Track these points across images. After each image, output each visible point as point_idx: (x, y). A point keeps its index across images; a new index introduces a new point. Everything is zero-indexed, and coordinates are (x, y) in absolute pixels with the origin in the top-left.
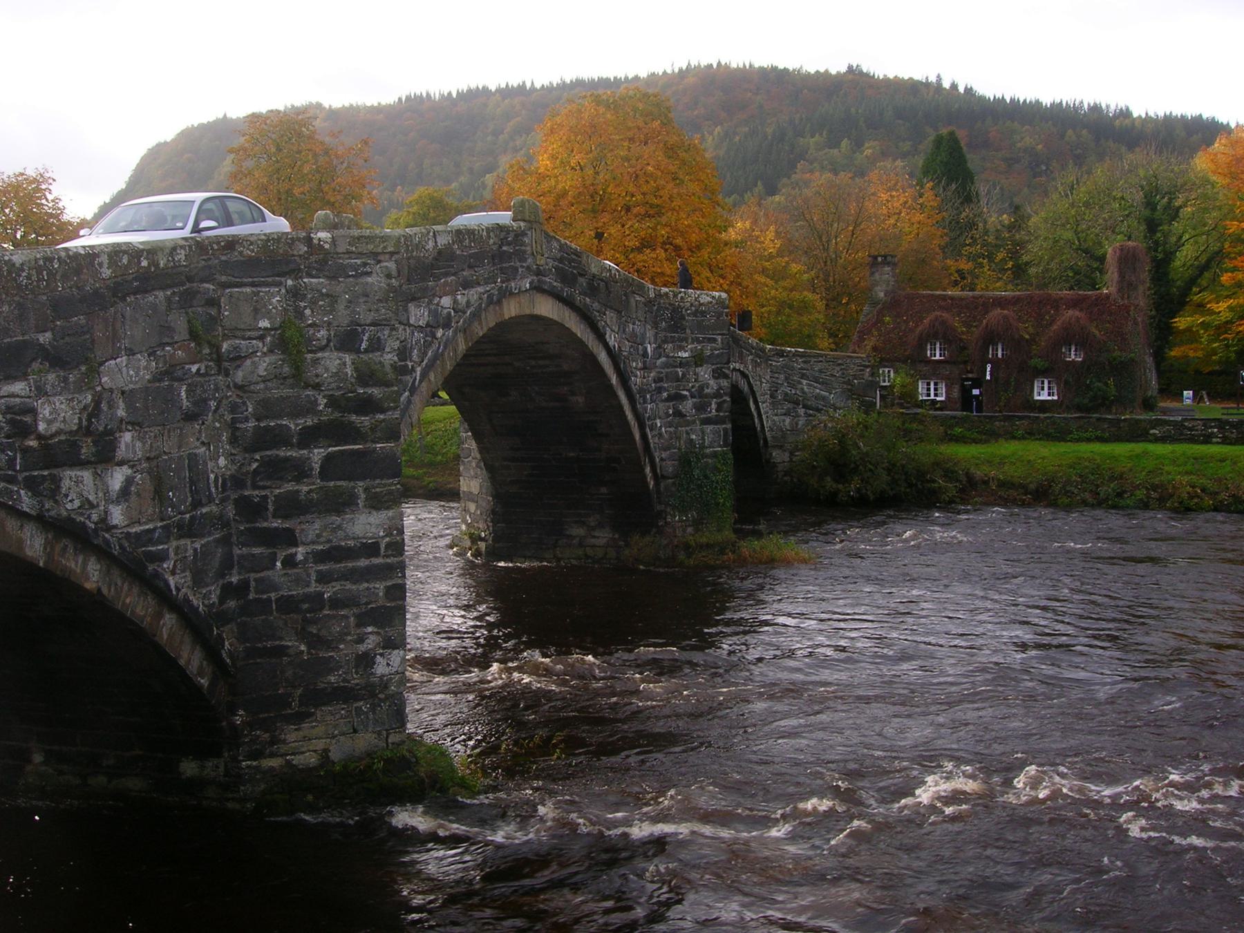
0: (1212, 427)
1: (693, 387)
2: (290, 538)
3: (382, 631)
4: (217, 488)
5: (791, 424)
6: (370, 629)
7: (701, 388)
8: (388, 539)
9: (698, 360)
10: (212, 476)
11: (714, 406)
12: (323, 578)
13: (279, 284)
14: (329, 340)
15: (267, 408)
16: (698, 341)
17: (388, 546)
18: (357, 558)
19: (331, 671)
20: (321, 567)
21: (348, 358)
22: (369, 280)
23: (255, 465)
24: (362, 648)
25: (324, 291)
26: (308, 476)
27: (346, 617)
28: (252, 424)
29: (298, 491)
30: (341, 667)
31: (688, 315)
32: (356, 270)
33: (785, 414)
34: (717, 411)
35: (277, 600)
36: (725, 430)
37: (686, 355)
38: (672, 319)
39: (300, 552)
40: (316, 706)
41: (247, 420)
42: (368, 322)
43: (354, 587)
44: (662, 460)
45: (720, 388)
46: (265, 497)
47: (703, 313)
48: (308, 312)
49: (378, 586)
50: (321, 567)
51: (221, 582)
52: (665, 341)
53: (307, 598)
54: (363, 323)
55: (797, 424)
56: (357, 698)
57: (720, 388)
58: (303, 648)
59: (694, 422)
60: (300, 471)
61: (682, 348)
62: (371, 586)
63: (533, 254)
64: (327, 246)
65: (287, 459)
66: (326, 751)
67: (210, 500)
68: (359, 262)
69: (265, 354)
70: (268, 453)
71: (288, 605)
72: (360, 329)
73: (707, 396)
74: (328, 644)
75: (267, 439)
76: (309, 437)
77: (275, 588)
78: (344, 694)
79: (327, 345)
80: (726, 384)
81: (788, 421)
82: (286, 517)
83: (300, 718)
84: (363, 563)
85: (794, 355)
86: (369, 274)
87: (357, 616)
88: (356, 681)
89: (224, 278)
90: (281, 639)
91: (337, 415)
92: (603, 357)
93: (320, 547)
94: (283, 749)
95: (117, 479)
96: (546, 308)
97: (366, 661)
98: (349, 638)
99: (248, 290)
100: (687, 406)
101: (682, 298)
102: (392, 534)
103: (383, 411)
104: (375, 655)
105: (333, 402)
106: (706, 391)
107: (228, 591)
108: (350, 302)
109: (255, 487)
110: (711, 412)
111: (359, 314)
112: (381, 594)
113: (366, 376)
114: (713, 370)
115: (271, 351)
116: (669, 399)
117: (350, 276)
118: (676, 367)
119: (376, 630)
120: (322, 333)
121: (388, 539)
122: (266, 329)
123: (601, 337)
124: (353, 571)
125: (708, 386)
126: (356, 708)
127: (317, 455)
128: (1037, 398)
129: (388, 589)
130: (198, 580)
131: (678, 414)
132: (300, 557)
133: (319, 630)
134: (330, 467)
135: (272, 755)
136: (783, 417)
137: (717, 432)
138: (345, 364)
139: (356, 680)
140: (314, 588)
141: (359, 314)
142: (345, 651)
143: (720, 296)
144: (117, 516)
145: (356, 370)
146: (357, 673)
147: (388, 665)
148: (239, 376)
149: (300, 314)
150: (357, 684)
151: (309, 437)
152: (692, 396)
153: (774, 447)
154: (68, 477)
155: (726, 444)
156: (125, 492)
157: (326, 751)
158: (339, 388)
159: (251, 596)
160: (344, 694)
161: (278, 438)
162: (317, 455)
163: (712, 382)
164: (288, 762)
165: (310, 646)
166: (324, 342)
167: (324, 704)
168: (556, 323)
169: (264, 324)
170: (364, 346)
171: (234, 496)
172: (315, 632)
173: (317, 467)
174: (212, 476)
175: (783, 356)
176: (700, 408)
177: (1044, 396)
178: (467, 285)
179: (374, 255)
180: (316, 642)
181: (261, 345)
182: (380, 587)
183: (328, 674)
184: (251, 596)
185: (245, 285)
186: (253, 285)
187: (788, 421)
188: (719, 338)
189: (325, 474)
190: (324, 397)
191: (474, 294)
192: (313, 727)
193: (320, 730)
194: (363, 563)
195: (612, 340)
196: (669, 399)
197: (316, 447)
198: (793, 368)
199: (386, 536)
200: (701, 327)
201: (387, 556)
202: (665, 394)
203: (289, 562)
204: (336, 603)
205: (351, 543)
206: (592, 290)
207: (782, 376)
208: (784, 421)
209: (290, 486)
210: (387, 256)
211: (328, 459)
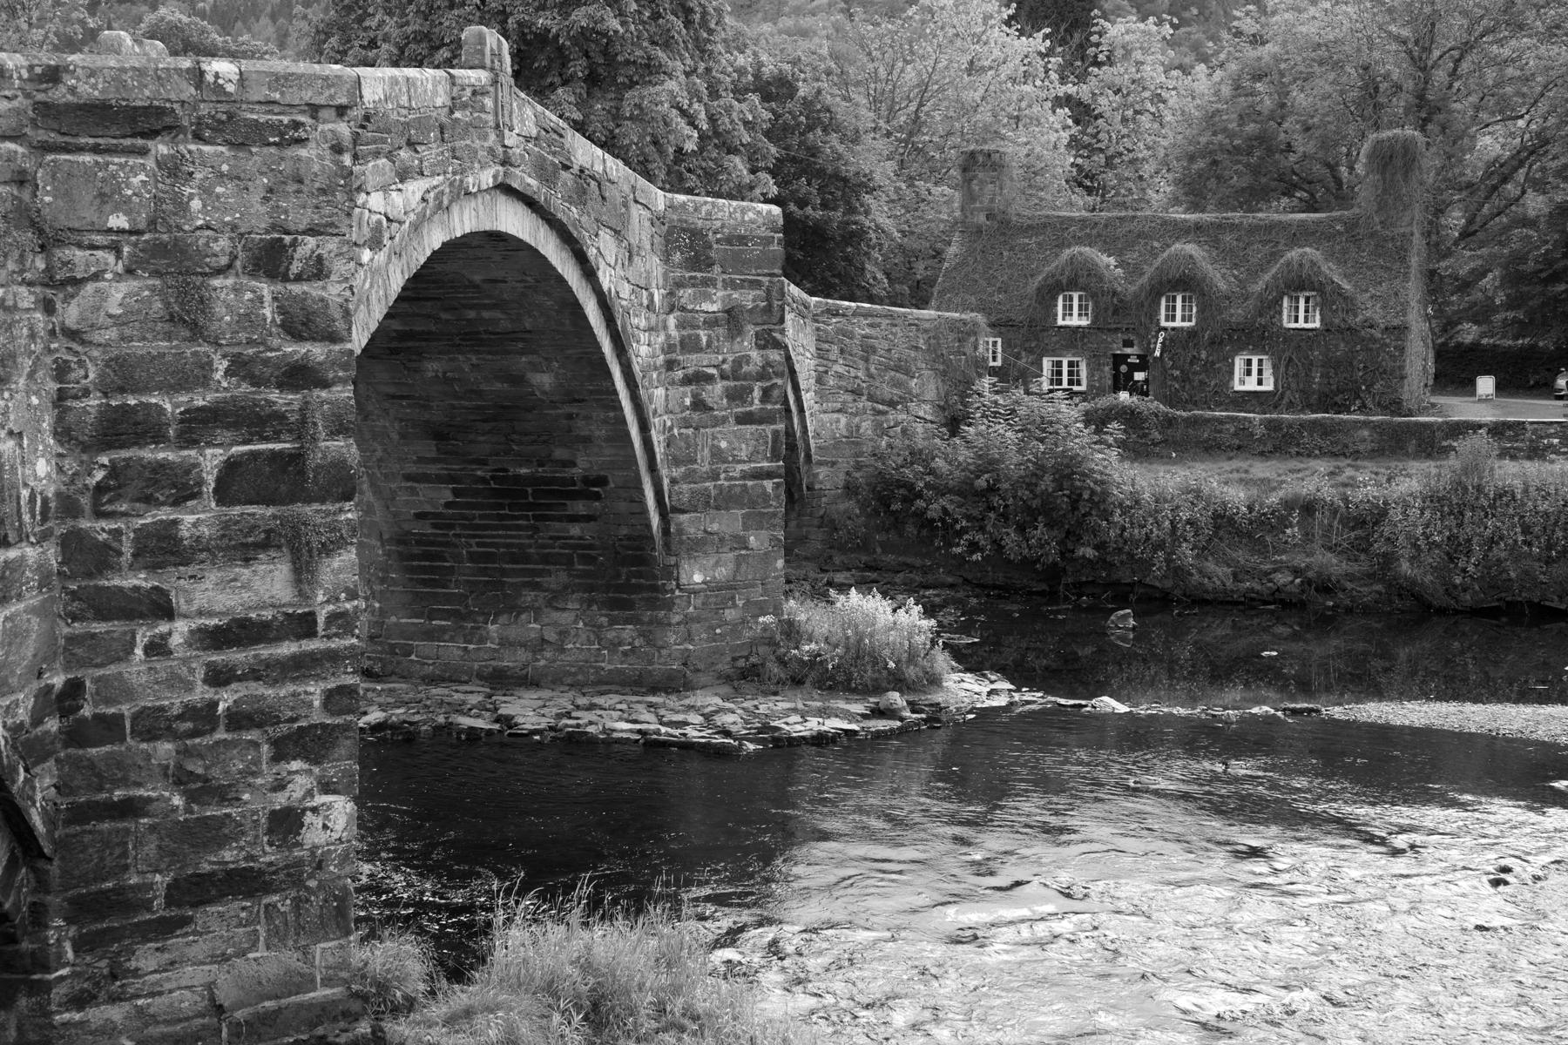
0: (1549, 436)
1: (724, 361)
2: (162, 609)
3: (316, 770)
4: (33, 516)
5: (848, 425)
6: (296, 765)
7: (738, 363)
8: (331, 607)
9: (732, 318)
10: (25, 493)
11: (757, 393)
12: (219, 677)
13: (143, 152)
14: (234, 257)
15: (122, 374)
16: (732, 285)
17: (332, 618)
18: (278, 639)
19: (222, 843)
20: (216, 658)
21: (266, 289)
22: (303, 152)
23: (99, 475)
24: (280, 800)
25: (225, 168)
26: (193, 496)
27: (255, 745)
28: (94, 402)
29: (175, 522)
30: (243, 833)
31: (718, 241)
32: (281, 135)
33: (839, 411)
34: (762, 401)
35: (136, 717)
36: (776, 433)
37: (714, 308)
38: (691, 248)
39: (179, 631)
40: (195, 905)
41: (86, 393)
42: (301, 227)
43: (270, 692)
44: (673, 481)
45: (768, 364)
46: (117, 533)
47: (742, 240)
48: (196, 204)
49: (311, 689)
50: (216, 658)
51: (36, 685)
52: (679, 284)
53: (189, 712)
54: (292, 227)
55: (858, 427)
56: (268, 888)
57: (768, 364)
58: (177, 801)
59: (724, 420)
60: (184, 490)
61: (708, 297)
62: (300, 689)
63: (498, 126)
64: (230, 88)
65: (162, 466)
66: (210, 986)
67: (22, 537)
68: (286, 119)
69: (118, 277)
70: (125, 454)
71: (152, 725)
72: (287, 239)
73: (746, 377)
74: (224, 795)
76: (196, 427)
77: (129, 694)
78: (246, 883)
79: (230, 266)
80: (778, 358)
81: (843, 420)
82: (153, 568)
83: (165, 928)
84: (287, 649)
85: (855, 314)
86: (300, 142)
87: (276, 743)
88: (267, 859)
89: (42, 135)
90: (139, 785)
91: (245, 388)
93: (214, 621)
94: (135, 985)
96: (514, 221)
97: (287, 823)
98: (259, 781)
99: (87, 158)
100: (715, 392)
101: (709, 213)
102: (338, 599)
103: (326, 385)
104: (304, 810)
105: (239, 367)
106: (745, 368)
108: (271, 191)
109: (99, 514)
110: (752, 403)
111: (286, 212)
112: (317, 703)
113: (300, 323)
114: (757, 334)
115: (130, 271)
116: (687, 381)
117: (269, 144)
118: (699, 327)
119: (306, 766)
120: (223, 243)
121: (331, 607)
122: (121, 231)
124: (269, 664)
125: (748, 359)
126: (267, 906)
127: (210, 460)
128: (1238, 387)
129: (329, 697)
131: (699, 405)
132: (176, 640)
133: (207, 768)
134: (232, 483)
135: (114, 999)
136: (835, 416)
137: (761, 437)
138: (261, 299)
139: (270, 856)
140: (201, 693)
141: (286, 212)
142: (255, 803)
143: (769, 212)
145: (282, 310)
146: (271, 844)
147: (325, 827)
148: (71, 314)
149: (182, 206)
150: (271, 864)
151: (196, 427)
152: (723, 377)
153: (820, 463)
155: (775, 456)
157: (210, 986)
158: (250, 342)
159: (87, 711)
160: (246, 883)
161: (146, 428)
162: (210, 460)
163: (755, 354)
164: (140, 1011)
165: (191, 797)
166: (224, 261)
167: (210, 902)
168: (529, 247)
169: (118, 221)
170: (295, 268)
171: (59, 531)
172: (200, 771)
173: (211, 480)
174: (25, 493)
175: (837, 315)
176: (736, 396)
177: (1251, 385)
179: (314, 110)
180: (201, 790)
181: (111, 258)
182: (315, 691)
183: (221, 846)
184: (87, 711)
185: (80, 149)
186: (96, 149)
187: (843, 420)
188: (765, 279)
189: (224, 494)
190: (224, 356)
191: (415, 189)
192: (188, 944)
193: (201, 948)
194: (287, 649)
195: (606, 279)
196: (687, 381)
197: (209, 444)
198: (851, 336)
199: (328, 602)
201: (329, 637)
202: (680, 374)
203: (157, 648)
204: (238, 720)
205: (268, 614)
207: (835, 348)
208: (838, 421)
209: (164, 514)
210: (332, 113)
211: (231, 468)
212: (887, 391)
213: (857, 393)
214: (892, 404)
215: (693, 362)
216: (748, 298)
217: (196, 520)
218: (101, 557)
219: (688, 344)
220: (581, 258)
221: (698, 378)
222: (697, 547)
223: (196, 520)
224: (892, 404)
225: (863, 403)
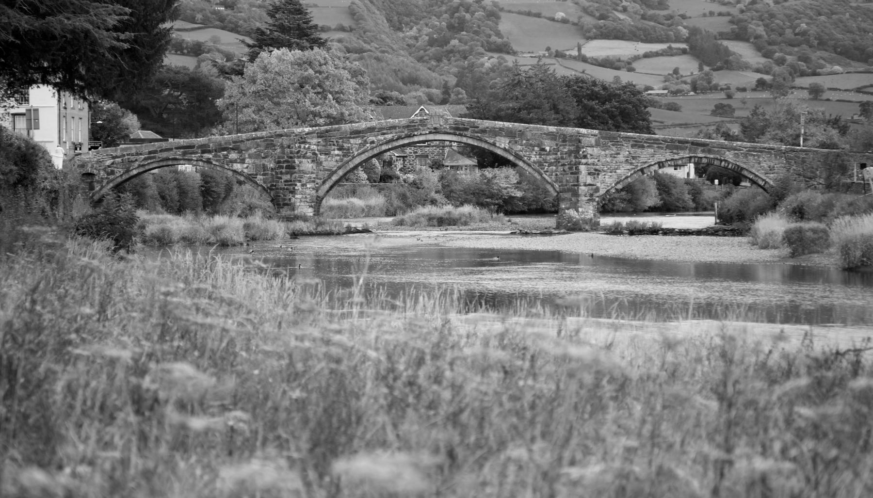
2: (281, 178)
9: (570, 153)
15: (279, 157)
71: (281, 189)
75: (279, 162)
76: (284, 162)
92: (499, 152)
95: (245, 165)
97: (290, 199)
100: (566, 168)
107: (272, 185)
113: (291, 153)
123: (494, 145)
130: (265, 182)
142: (288, 197)
144: (245, 171)
151: (284, 162)
154: (235, 165)
156: (247, 167)
176: (570, 168)
178: (384, 134)
198: (799, 157)
200: (571, 141)
206: (483, 131)
212: (809, 174)
213: (799, 175)
214: (811, 178)
215: (562, 161)
216: (572, 148)
217: (284, 171)
218: (277, 173)
219: (562, 158)
220: (486, 142)
221: (563, 165)
222: (564, 200)
223: (284, 171)
224: (811, 178)
225: (802, 178)
